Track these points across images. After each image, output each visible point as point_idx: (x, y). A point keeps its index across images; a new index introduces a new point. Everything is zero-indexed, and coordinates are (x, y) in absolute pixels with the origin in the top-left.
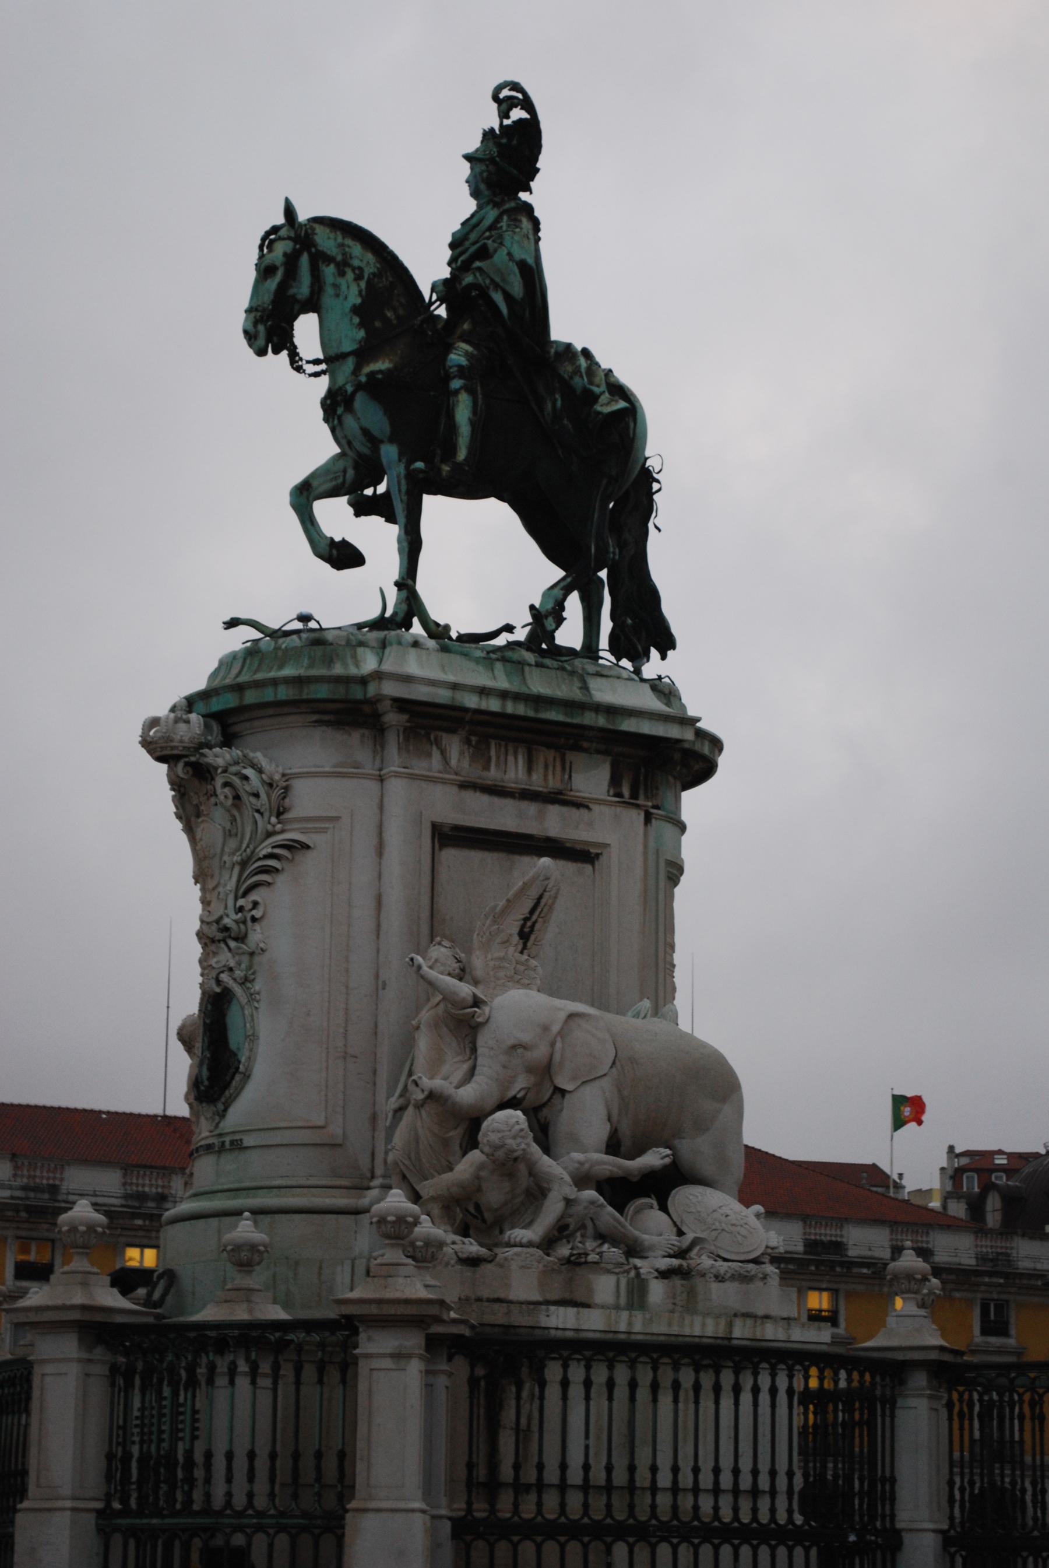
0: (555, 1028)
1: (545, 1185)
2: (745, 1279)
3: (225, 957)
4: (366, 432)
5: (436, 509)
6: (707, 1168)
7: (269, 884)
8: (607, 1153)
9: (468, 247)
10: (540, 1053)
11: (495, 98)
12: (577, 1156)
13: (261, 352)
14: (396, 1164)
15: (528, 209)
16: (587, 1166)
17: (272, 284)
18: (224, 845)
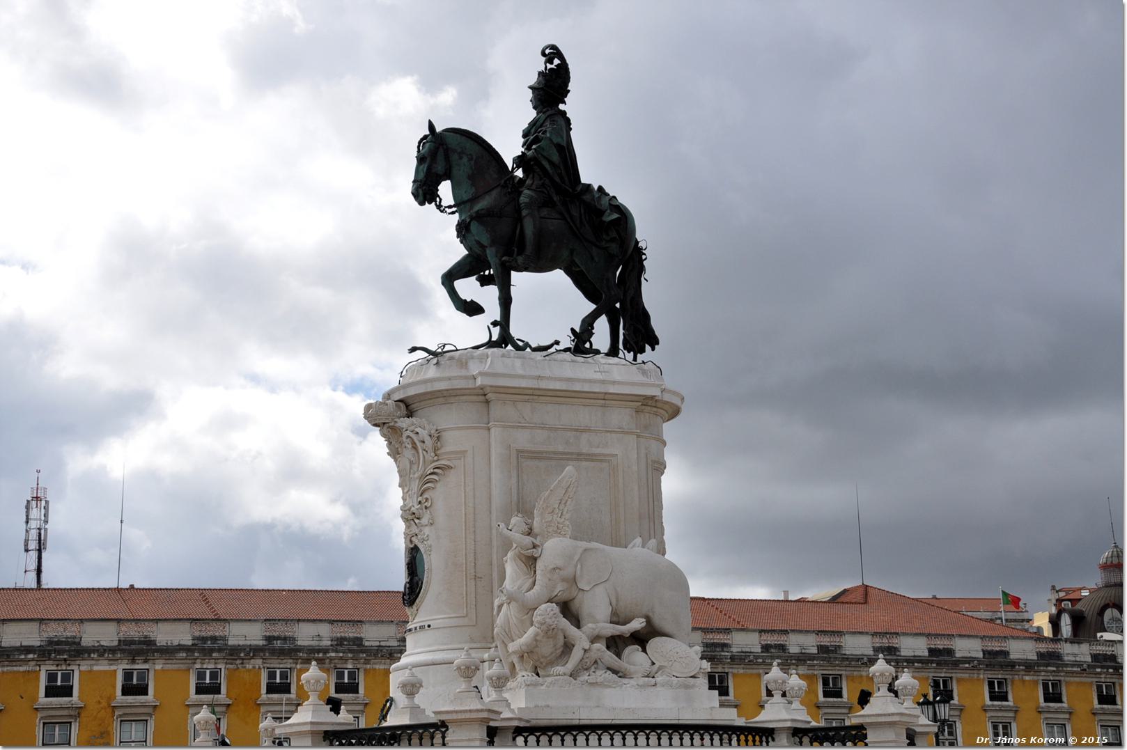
0: (576, 558)
2: (687, 687)
4: (478, 243)
5: (519, 279)
6: (666, 626)
9: (532, 134)
10: (568, 572)
11: (543, 54)
12: (590, 625)
13: (422, 204)
15: (564, 113)
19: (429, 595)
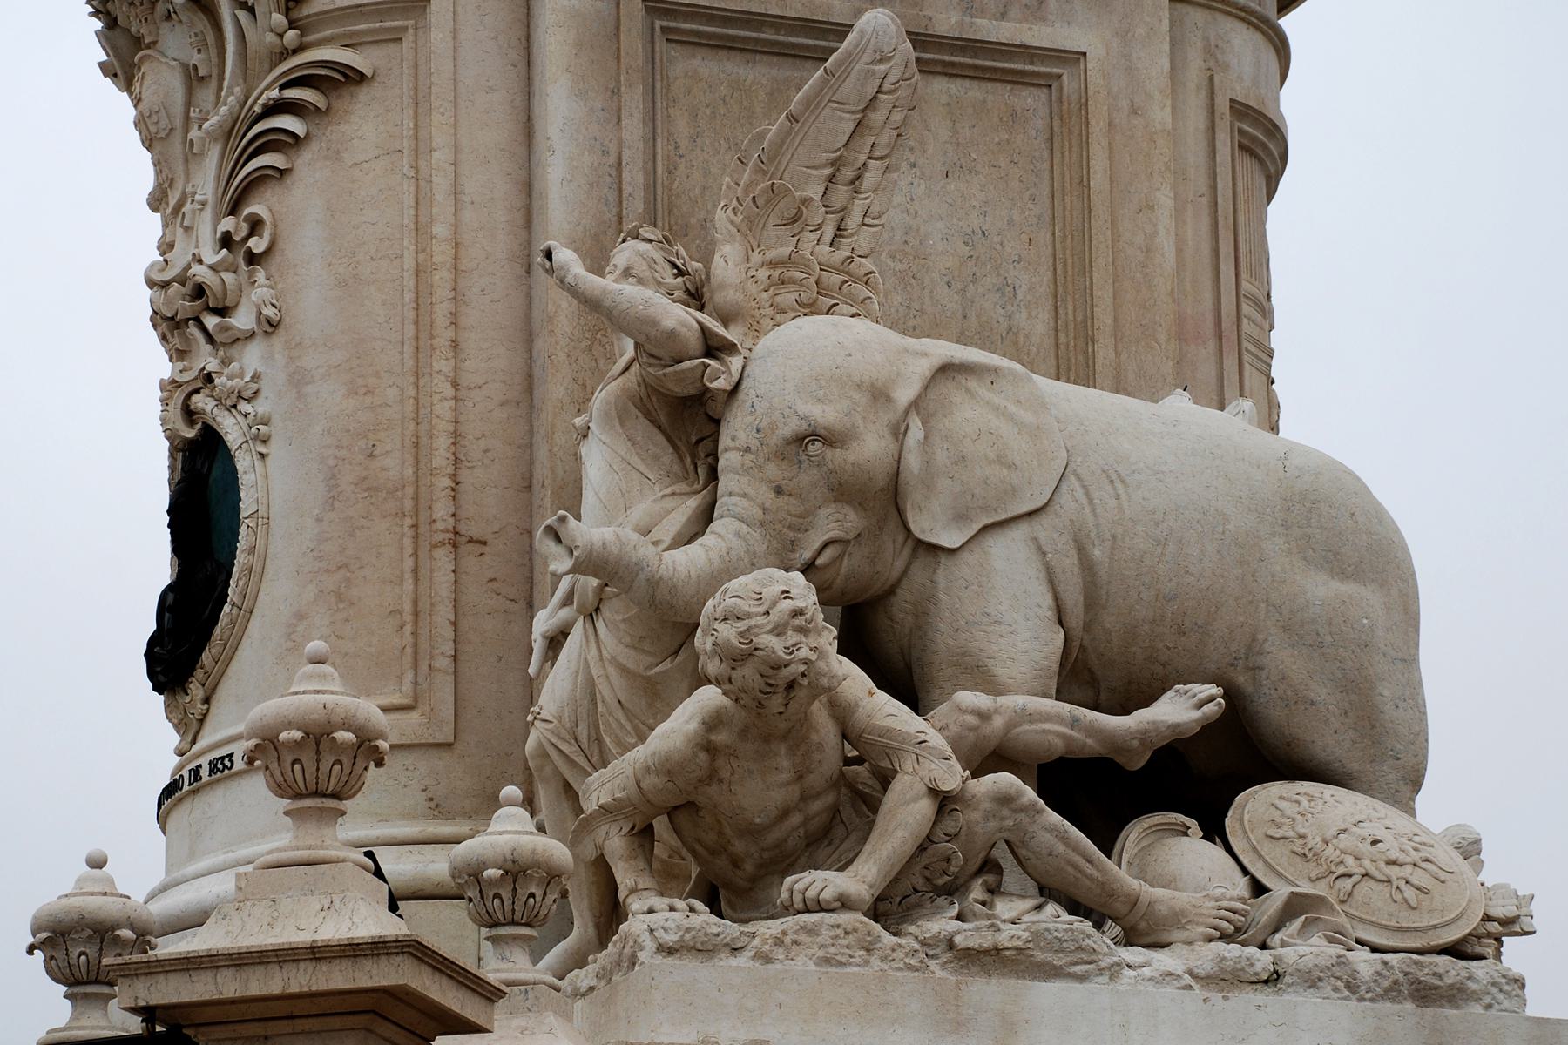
0: (904, 395)
1: (885, 764)
2: (1425, 994)
6: (1327, 737)
7: (283, 173)
8: (1059, 697)
12: (967, 698)
14: (542, 754)
16: (998, 722)
18: (188, 104)
19: (255, 627)
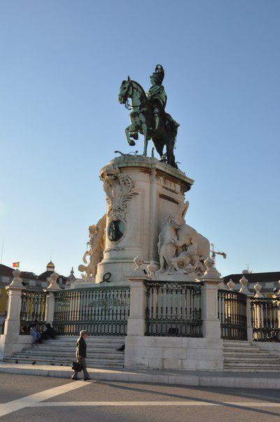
3: (118, 214)
17: (125, 91)
